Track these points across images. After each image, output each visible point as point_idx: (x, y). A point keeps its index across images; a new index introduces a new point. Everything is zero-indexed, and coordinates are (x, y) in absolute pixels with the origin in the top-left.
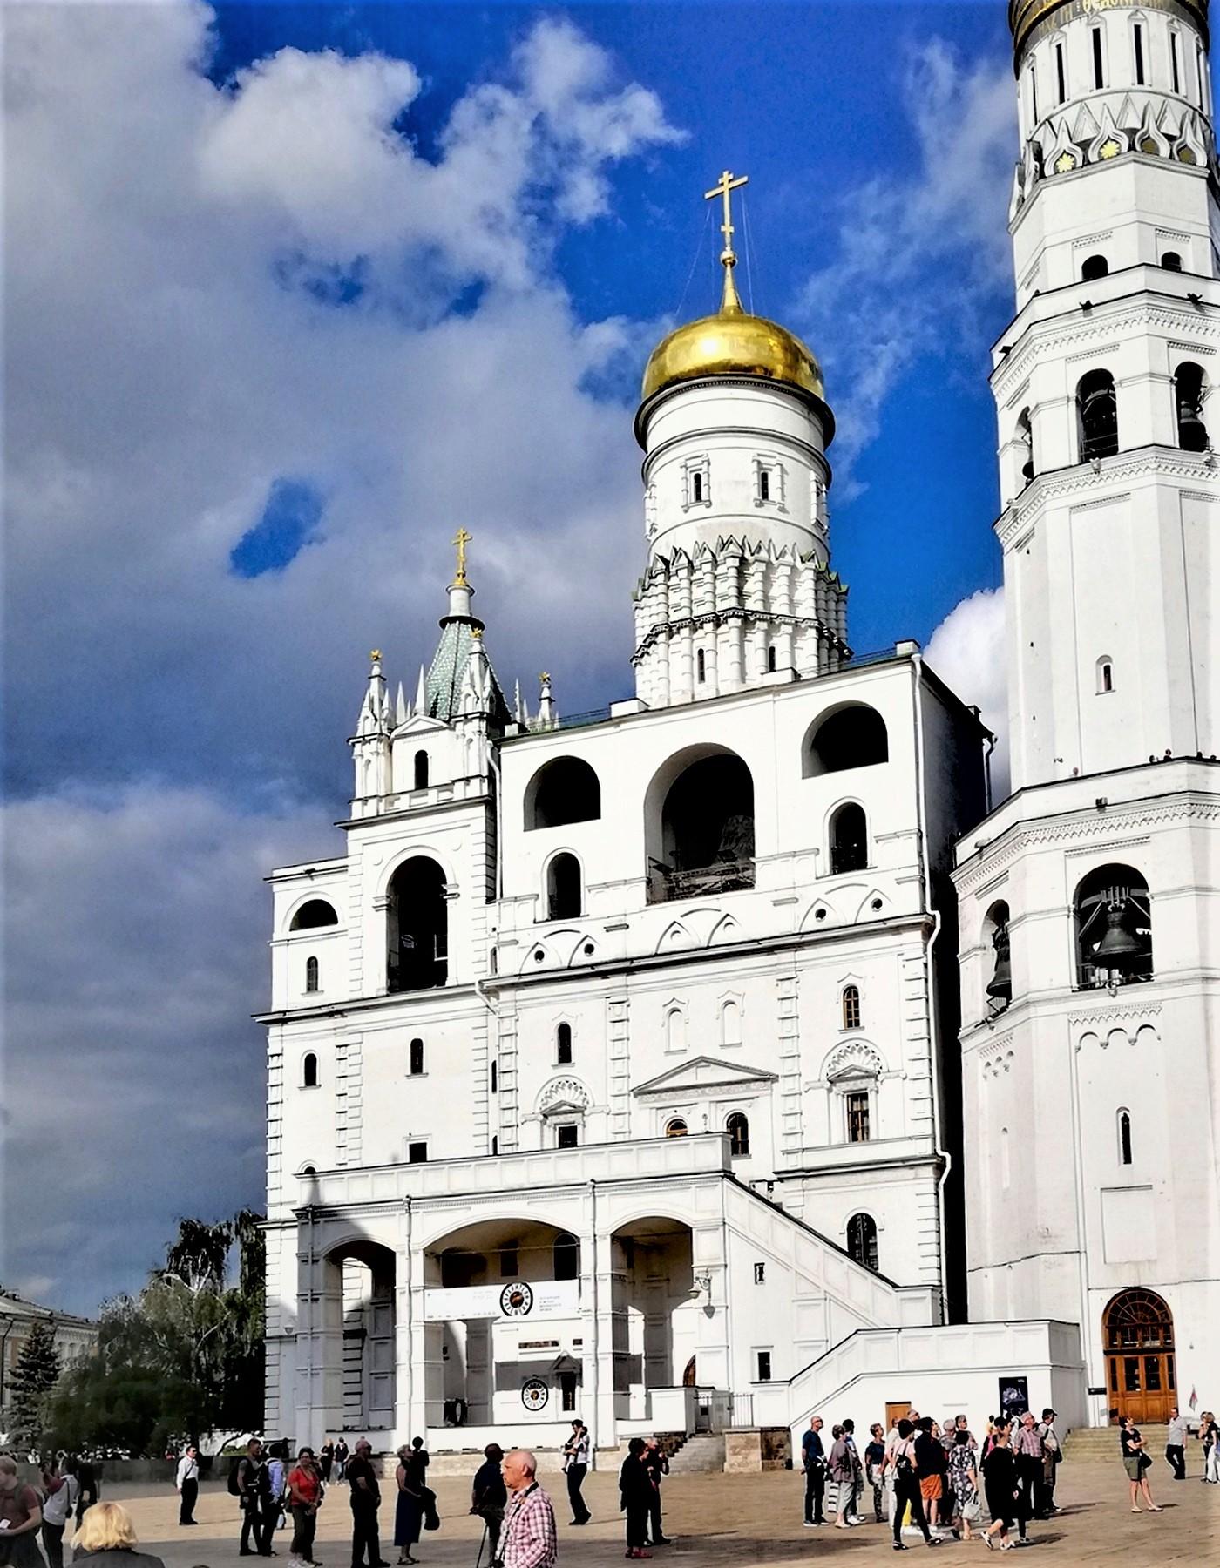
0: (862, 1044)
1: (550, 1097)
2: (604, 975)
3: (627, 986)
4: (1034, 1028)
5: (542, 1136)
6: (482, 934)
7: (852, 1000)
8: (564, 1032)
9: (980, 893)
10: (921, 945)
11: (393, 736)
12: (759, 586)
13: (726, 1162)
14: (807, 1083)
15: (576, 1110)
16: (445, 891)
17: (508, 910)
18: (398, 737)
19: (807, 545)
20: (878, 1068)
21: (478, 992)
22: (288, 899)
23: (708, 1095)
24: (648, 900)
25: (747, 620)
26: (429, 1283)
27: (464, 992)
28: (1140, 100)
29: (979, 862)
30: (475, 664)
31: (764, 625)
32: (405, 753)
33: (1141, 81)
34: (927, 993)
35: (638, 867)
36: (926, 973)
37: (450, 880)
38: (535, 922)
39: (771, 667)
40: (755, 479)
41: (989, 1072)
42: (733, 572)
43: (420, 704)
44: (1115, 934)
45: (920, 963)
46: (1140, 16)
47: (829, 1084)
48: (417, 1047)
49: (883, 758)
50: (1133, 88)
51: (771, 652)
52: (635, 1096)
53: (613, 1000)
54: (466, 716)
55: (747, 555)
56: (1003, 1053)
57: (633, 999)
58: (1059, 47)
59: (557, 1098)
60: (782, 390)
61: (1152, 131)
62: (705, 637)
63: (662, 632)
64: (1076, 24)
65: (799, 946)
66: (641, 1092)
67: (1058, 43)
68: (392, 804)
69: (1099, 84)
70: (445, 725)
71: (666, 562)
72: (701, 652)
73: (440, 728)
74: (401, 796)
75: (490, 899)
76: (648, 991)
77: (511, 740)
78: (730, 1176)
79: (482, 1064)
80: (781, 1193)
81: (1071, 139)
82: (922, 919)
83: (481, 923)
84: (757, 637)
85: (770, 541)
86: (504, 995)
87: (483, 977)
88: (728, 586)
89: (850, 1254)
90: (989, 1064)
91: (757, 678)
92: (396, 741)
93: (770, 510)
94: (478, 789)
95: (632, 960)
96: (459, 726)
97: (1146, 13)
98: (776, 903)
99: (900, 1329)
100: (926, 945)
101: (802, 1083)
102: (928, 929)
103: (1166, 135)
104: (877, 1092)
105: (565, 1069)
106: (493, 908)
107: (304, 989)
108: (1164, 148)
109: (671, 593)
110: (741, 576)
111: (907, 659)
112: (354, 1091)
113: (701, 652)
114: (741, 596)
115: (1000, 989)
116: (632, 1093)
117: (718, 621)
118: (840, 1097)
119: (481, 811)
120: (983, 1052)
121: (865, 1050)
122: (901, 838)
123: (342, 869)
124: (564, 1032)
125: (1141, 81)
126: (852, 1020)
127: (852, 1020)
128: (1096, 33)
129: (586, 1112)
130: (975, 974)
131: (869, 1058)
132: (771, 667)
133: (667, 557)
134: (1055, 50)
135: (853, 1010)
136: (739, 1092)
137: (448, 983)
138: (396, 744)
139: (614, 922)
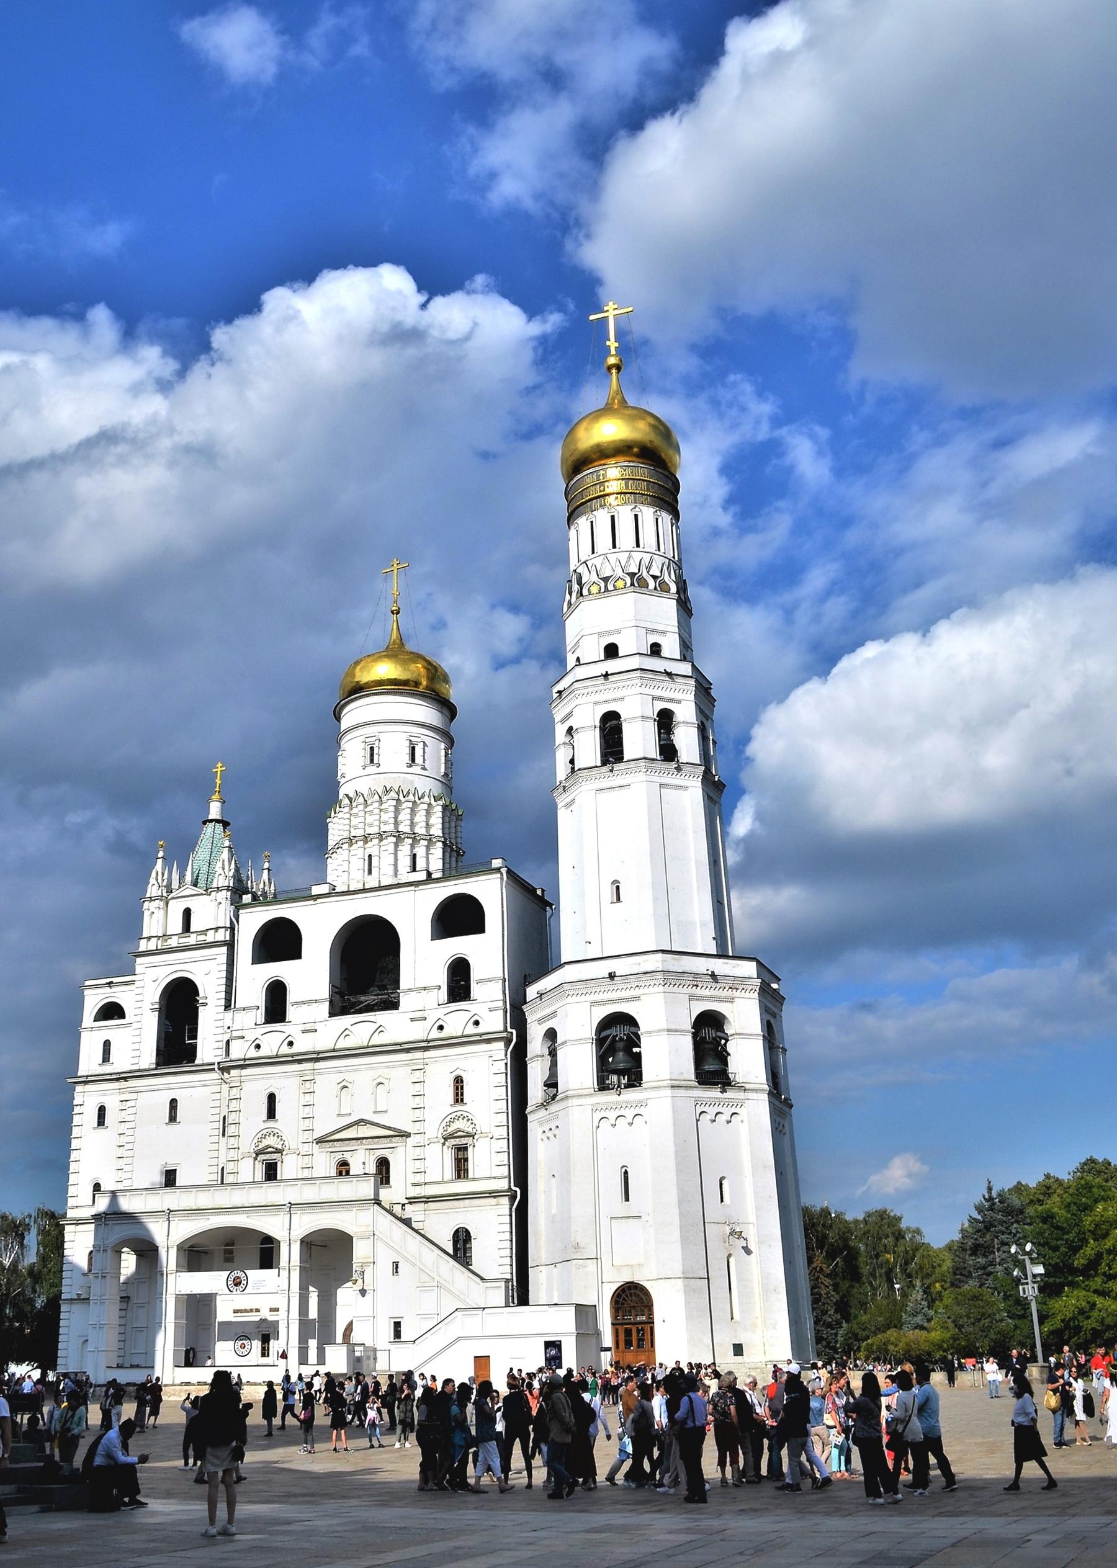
0: (465, 1114)
1: (261, 1142)
2: (300, 1062)
4: (570, 1113)
5: (254, 1168)
6: (221, 1030)
7: (459, 1085)
8: (272, 1098)
9: (541, 1021)
10: (503, 1052)
11: (169, 897)
12: (409, 817)
13: (377, 1193)
16: (198, 1001)
17: (239, 1016)
18: (172, 898)
20: (475, 1131)
21: (216, 1069)
22: (93, 1001)
23: (365, 1144)
24: (330, 1013)
25: (399, 837)
26: (180, 1268)
27: (207, 1068)
28: (637, 556)
30: (225, 854)
32: (176, 909)
33: (638, 545)
34: (507, 1083)
36: (506, 1069)
37: (201, 994)
38: (256, 1025)
39: (414, 869)
40: (407, 751)
41: (544, 1136)
42: (392, 809)
43: (188, 878)
44: (621, 1055)
46: (637, 509)
48: (173, 1103)
49: (483, 931)
51: (414, 857)
52: (317, 1143)
55: (401, 797)
58: (592, 522)
59: (265, 1143)
60: (426, 696)
61: (645, 574)
62: (373, 848)
64: (601, 511)
65: (426, 1049)
68: (166, 940)
69: (614, 546)
70: (204, 892)
71: (350, 799)
72: (370, 856)
73: (202, 894)
74: (173, 937)
75: (227, 1007)
76: (328, 1075)
77: (247, 906)
78: (377, 1202)
79: (216, 1118)
82: (504, 1035)
83: (220, 1023)
84: (405, 849)
86: (233, 1072)
87: (219, 1059)
88: (388, 816)
89: (455, 1257)
90: (544, 1132)
91: (405, 876)
92: (171, 901)
93: (416, 769)
94: (223, 936)
95: (318, 1053)
97: (641, 507)
98: (412, 1020)
99: (484, 1308)
100: (506, 1051)
101: (426, 1139)
102: (508, 1041)
103: (652, 576)
104: (474, 1146)
105: (271, 1124)
106: (229, 1014)
107: (100, 1060)
108: (652, 584)
109: (352, 818)
110: (397, 811)
111: (498, 870)
112: (130, 1132)
113: (370, 856)
114: (396, 823)
115: (551, 1084)
116: (315, 1142)
117: (381, 836)
118: (450, 1149)
119: (224, 950)
120: (541, 1123)
121: (466, 1118)
123: (132, 982)
124: (272, 1098)
125: (638, 545)
126: (459, 1098)
127: (459, 1098)
128: (613, 517)
129: (284, 1153)
130: (536, 1073)
132: (414, 869)
133: (351, 795)
134: (590, 524)
137: (197, 1062)
138: (171, 903)
139: (308, 1027)
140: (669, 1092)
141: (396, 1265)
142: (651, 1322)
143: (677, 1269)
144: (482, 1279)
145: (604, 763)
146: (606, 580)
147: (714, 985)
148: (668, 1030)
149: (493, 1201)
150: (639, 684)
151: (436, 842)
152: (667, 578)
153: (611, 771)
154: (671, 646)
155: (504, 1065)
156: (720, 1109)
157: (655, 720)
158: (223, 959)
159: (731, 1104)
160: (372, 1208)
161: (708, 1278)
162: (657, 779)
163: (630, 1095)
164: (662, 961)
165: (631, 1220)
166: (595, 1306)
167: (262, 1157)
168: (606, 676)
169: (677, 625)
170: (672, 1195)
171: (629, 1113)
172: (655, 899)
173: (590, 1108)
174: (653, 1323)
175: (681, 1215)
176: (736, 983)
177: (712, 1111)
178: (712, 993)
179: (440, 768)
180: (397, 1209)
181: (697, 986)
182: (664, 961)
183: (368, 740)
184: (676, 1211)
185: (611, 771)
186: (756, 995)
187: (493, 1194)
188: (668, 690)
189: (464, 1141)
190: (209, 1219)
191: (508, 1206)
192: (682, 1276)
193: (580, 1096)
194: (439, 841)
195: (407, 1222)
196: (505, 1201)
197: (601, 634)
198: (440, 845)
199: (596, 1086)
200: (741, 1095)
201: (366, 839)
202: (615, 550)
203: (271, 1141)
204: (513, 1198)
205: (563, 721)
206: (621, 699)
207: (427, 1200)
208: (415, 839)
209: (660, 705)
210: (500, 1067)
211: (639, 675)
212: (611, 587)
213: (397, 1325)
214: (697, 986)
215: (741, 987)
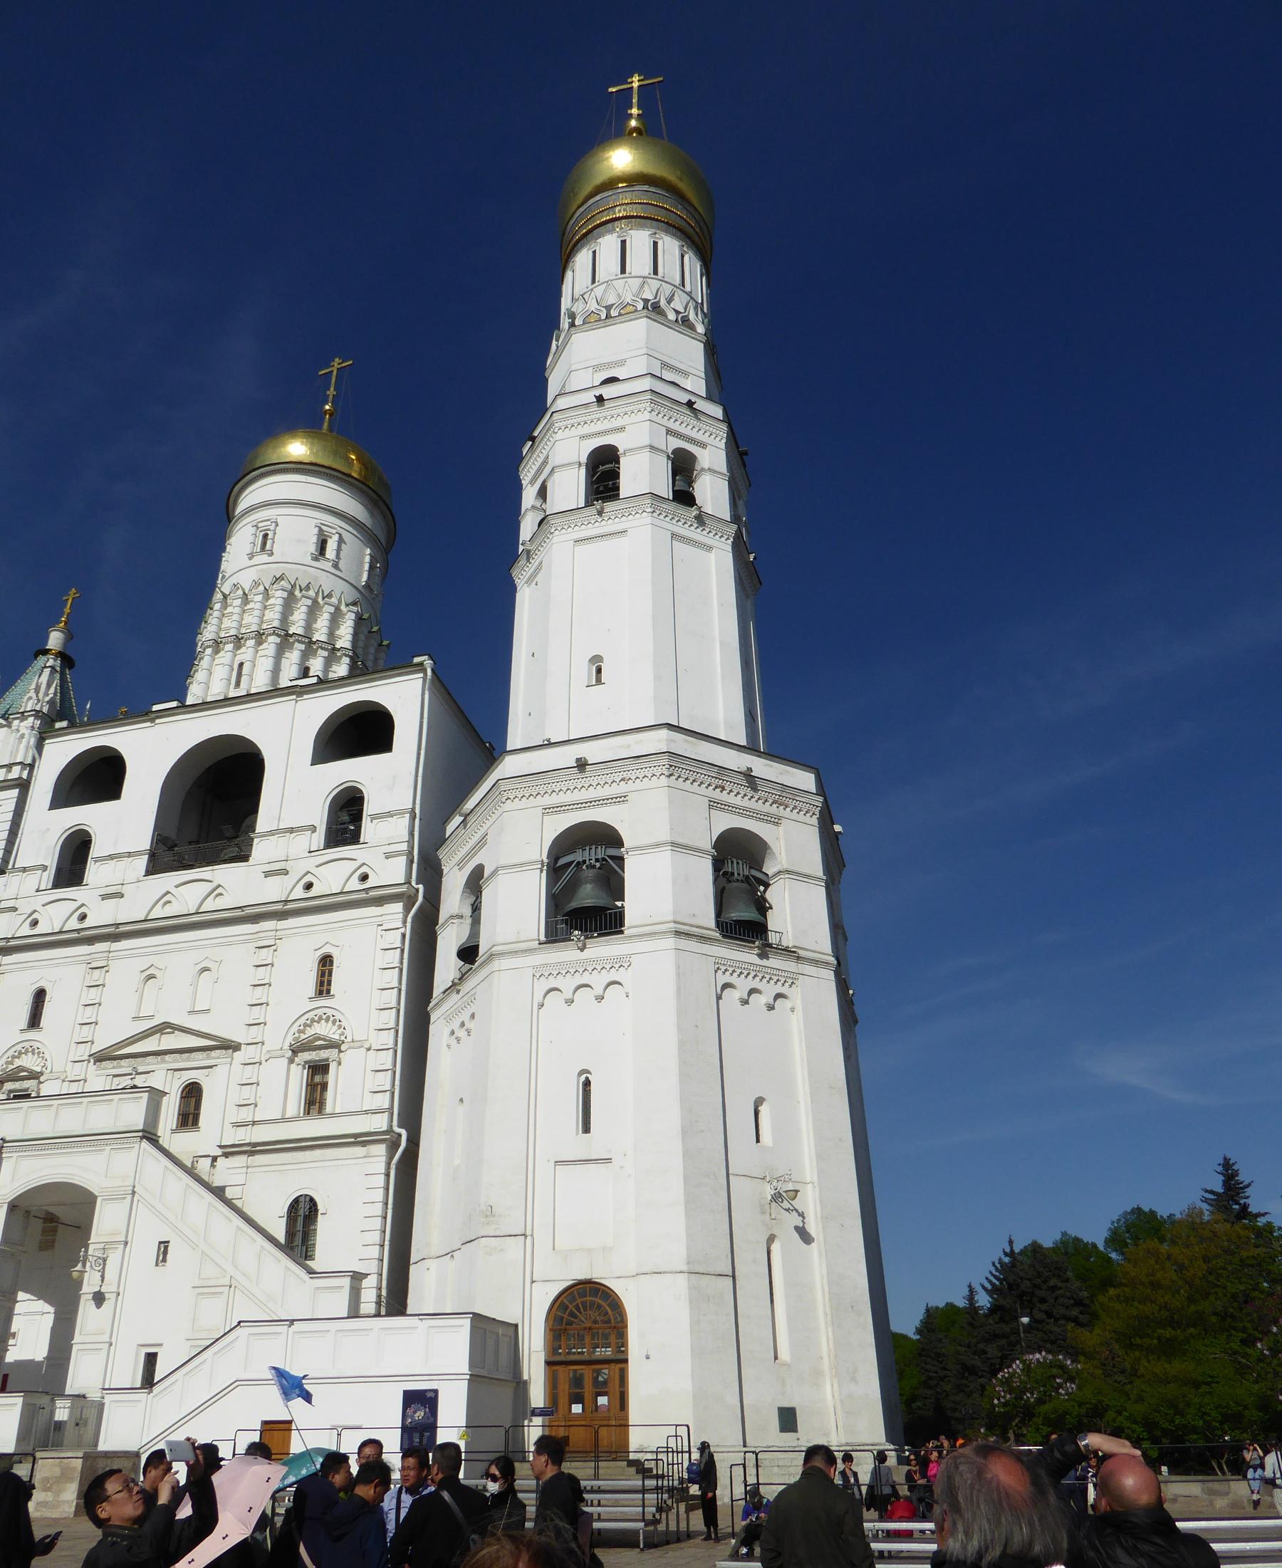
0: (330, 1012)
3: (110, 952)
8: (40, 996)
14: (268, 1051)
15: (35, 1076)
19: (352, 595)
20: (343, 1038)
25: (286, 640)
28: (655, 284)
29: (463, 831)
31: (302, 647)
33: (656, 272)
34: (402, 963)
41: (453, 1041)
45: (398, 934)
47: (290, 1052)
50: (650, 276)
53: (93, 965)
54: (23, 713)
56: (465, 1016)
57: (113, 965)
58: (594, 252)
59: (18, 1063)
61: (663, 303)
63: (209, 647)
66: (101, 1058)
67: (594, 249)
69: (623, 270)
72: (241, 665)
80: (227, 1173)
81: (598, 304)
82: (403, 889)
85: (321, 586)
90: (453, 1033)
96: (16, 723)
101: (264, 1051)
102: (409, 900)
105: (32, 1035)
108: (672, 316)
113: (241, 665)
115: (468, 954)
120: (448, 1020)
121: (332, 1019)
122: (395, 817)
124: (40, 996)
125: (656, 272)
126: (323, 987)
127: (323, 987)
129: (42, 1079)
131: (335, 1028)
135: (326, 979)
136: (200, 1059)
140: (671, 942)
141: (164, 1247)
142: (621, 1361)
143: (676, 1253)
144: (311, 1272)
145: (589, 503)
146: (609, 308)
147: (750, 793)
148: (673, 844)
149: (359, 1151)
150: (649, 409)
151: (340, 658)
152: (692, 317)
153: (600, 513)
154: (696, 383)
155: (399, 937)
156: (756, 984)
157: (668, 456)
158: (11, 805)
159: (775, 978)
160: (137, 1146)
161: (734, 1277)
162: (669, 526)
163: (602, 948)
164: (667, 740)
165: (592, 1166)
166: (516, 1326)
168: (600, 399)
169: (703, 370)
170: (672, 1118)
171: (598, 981)
172: (657, 678)
173: (530, 972)
174: (626, 1361)
175: (686, 1154)
176: (785, 794)
177: (743, 985)
178: (745, 803)
179: (360, 575)
180: (203, 1166)
181: (723, 789)
182: (670, 741)
183: (260, 525)
184: (677, 1146)
185: (600, 513)
186: (814, 821)
187: (360, 1140)
188: (686, 425)
189: (323, 1054)
191: (384, 1159)
192: (685, 1268)
193: (515, 953)
194: (346, 656)
195: (219, 1192)
196: (381, 1150)
197: (597, 368)
198: (346, 660)
199: (543, 938)
200: (791, 966)
201: (238, 641)
202: (623, 276)
204: (393, 1146)
205: (532, 482)
206: (621, 429)
207: (253, 1149)
208: (310, 646)
209: (675, 443)
210: (394, 939)
211: (649, 397)
212: (614, 313)
213: (151, 1359)
214: (723, 789)
215: (792, 804)
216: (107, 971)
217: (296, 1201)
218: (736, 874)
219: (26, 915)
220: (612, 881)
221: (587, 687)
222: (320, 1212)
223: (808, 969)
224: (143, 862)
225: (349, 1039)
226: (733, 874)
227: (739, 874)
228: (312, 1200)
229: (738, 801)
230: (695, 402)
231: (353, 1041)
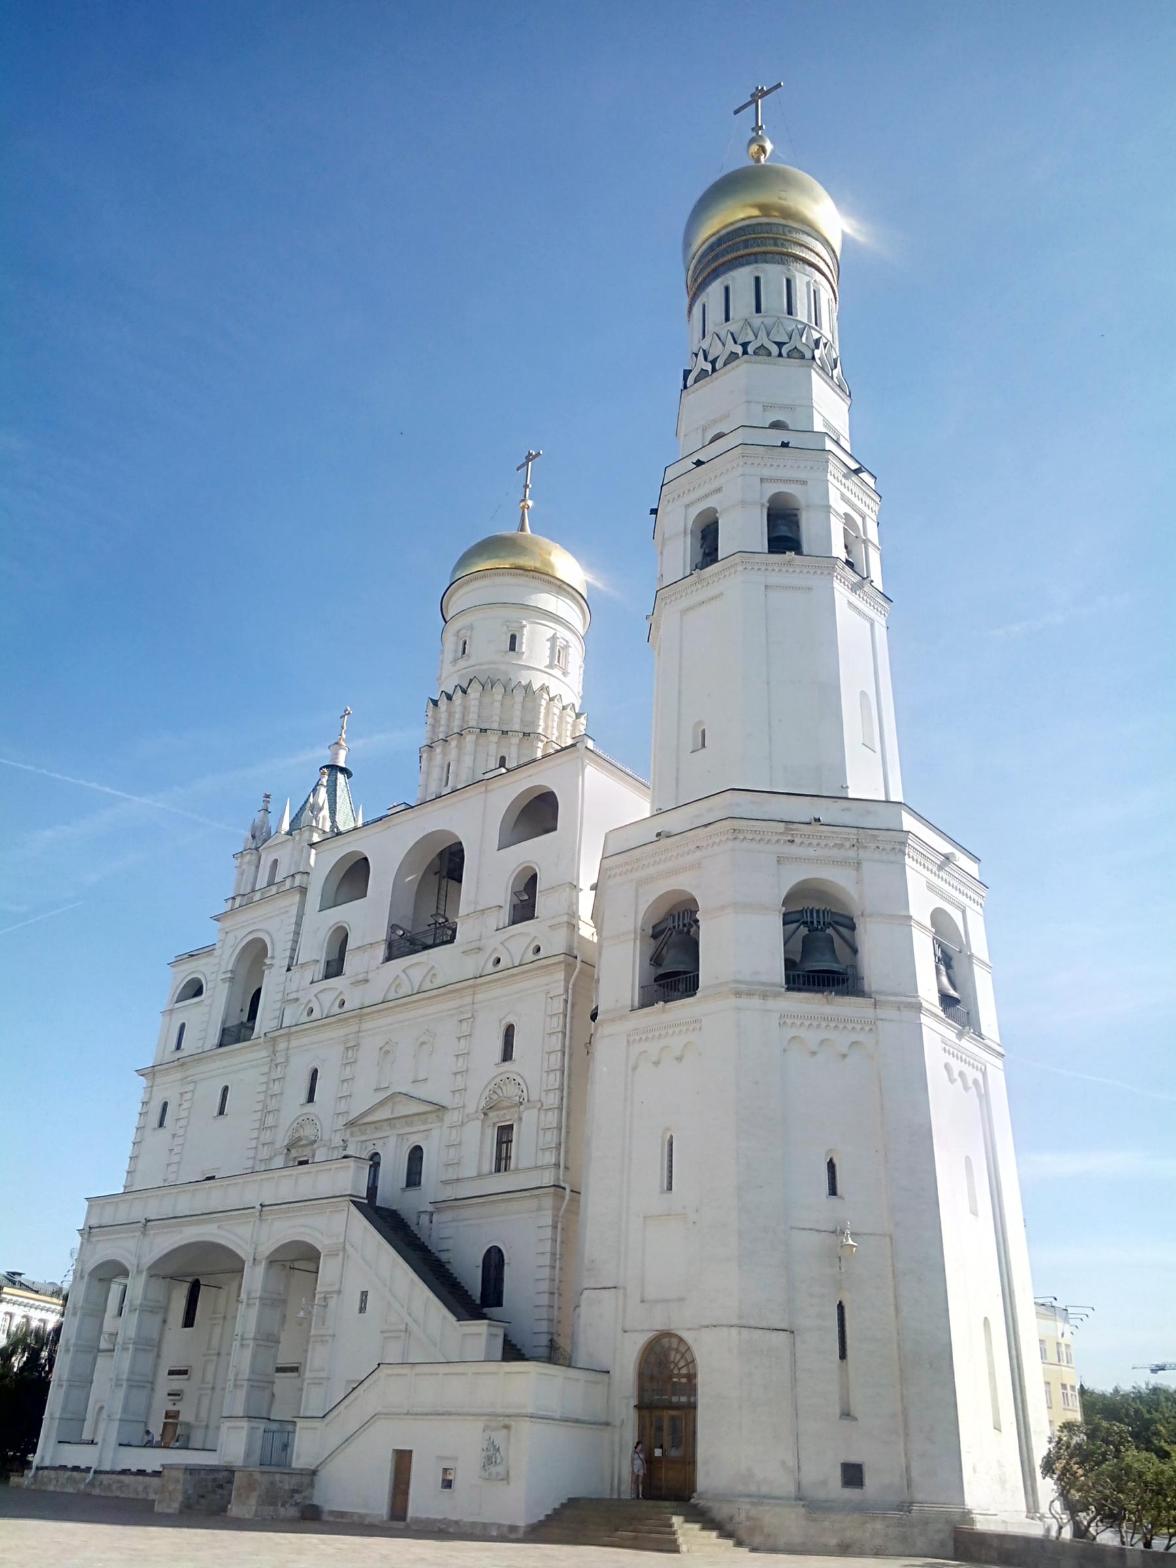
0: (512, 1076)
10: (562, 983)
20: (521, 1100)
33: (758, 310)
35: (383, 934)
47: (483, 1115)
53: (348, 1045)
96: (297, 838)
105: (309, 1108)
119: (297, 898)
125: (758, 310)
126: (507, 1055)
127: (507, 1055)
128: (727, 289)
129: (315, 1146)
139: (361, 977)
150: (741, 464)
167: (294, 1153)
168: (699, 463)
190: (181, 1232)
196: (548, 1202)
200: (869, 1013)
203: (308, 1132)
206: (719, 490)
209: (772, 489)
215: (873, 846)
216: (357, 1050)
217: (489, 1251)
218: (815, 923)
219: (303, 1006)
220: (691, 948)
221: (693, 752)
222: (506, 1261)
223: (891, 1013)
224: (381, 951)
225: (526, 1100)
226: (812, 923)
227: (819, 922)
228: (500, 1251)
229: (810, 852)
230: (789, 443)
231: (528, 1101)
